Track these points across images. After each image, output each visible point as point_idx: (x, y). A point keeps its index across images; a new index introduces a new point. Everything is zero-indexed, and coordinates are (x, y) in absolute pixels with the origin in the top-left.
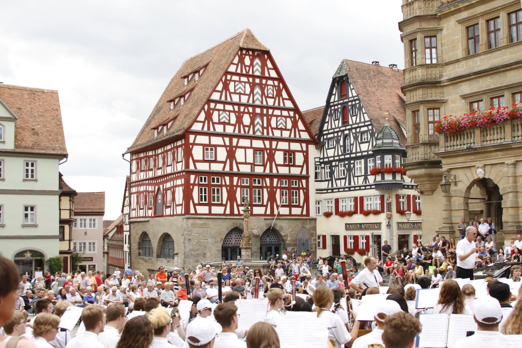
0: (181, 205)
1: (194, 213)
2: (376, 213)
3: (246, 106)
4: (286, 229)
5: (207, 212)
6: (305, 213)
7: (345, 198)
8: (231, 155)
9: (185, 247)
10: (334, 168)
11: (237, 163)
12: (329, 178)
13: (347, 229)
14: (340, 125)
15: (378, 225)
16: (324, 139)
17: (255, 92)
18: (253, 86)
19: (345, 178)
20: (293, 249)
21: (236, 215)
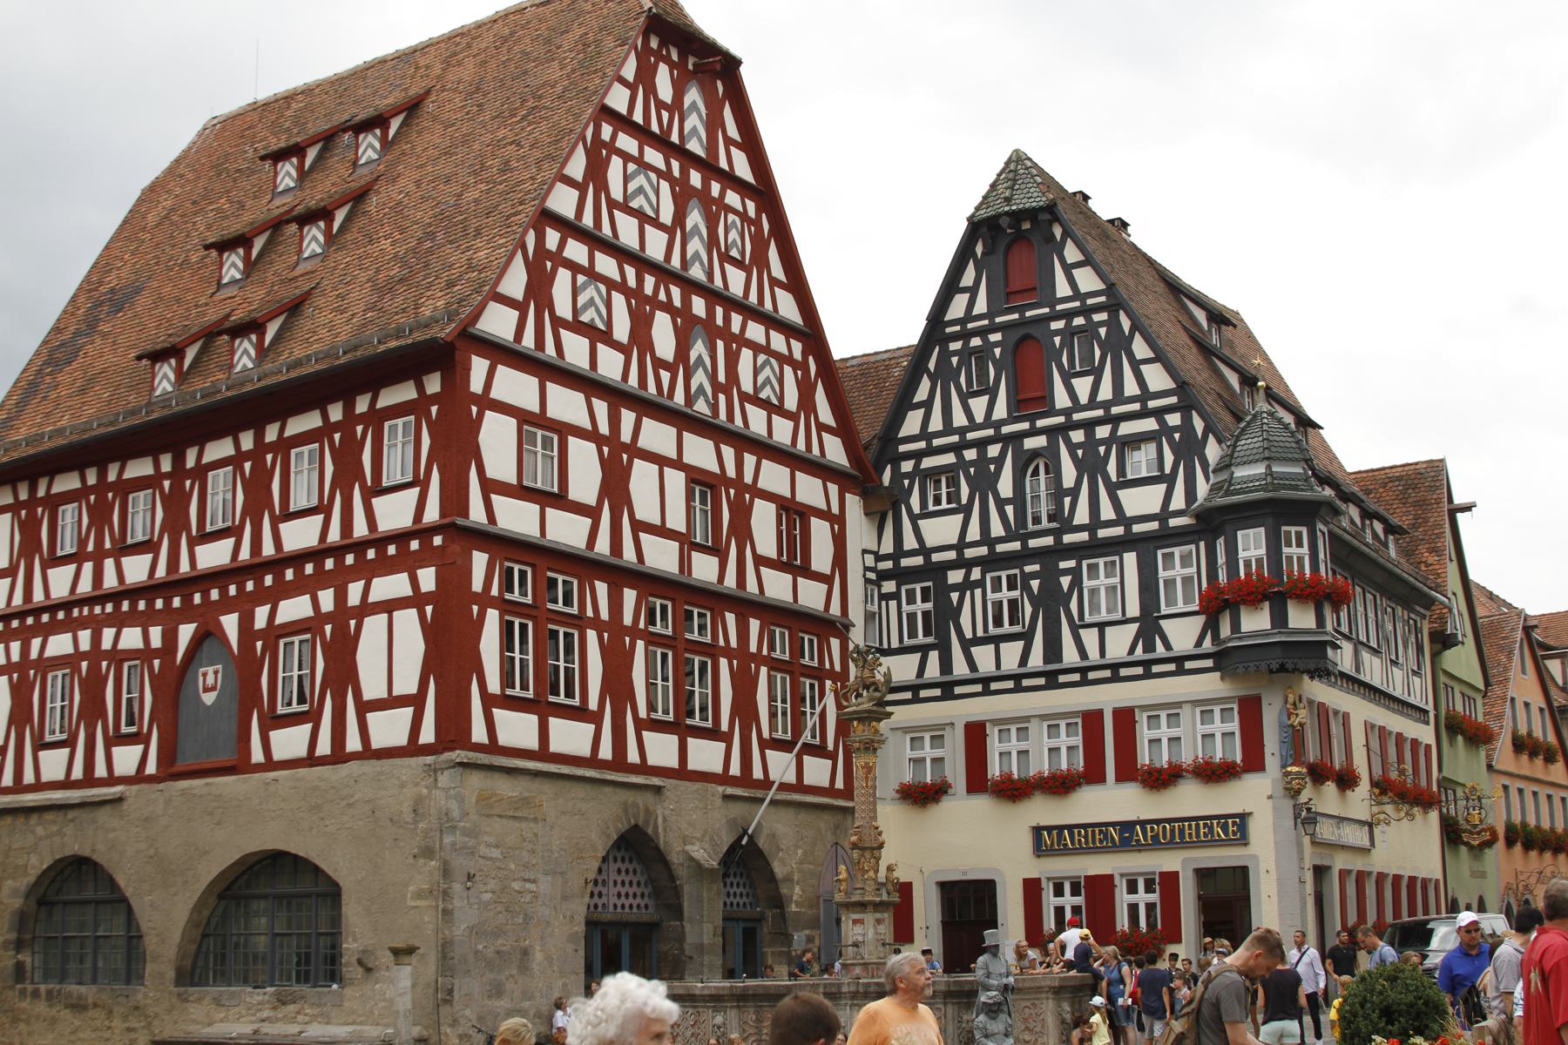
0: (417, 701)
1: (486, 741)
2: (1214, 773)
3: (663, 273)
4: (791, 848)
5: (533, 743)
6: (839, 784)
7: (1027, 719)
8: (615, 486)
9: (446, 912)
10: (955, 596)
11: (639, 527)
12: (921, 639)
13: (1040, 850)
14: (1000, 411)
15: (1237, 826)
16: (897, 476)
17: (689, 225)
18: (683, 197)
19: (1027, 637)
20: (810, 939)
21: (633, 769)
